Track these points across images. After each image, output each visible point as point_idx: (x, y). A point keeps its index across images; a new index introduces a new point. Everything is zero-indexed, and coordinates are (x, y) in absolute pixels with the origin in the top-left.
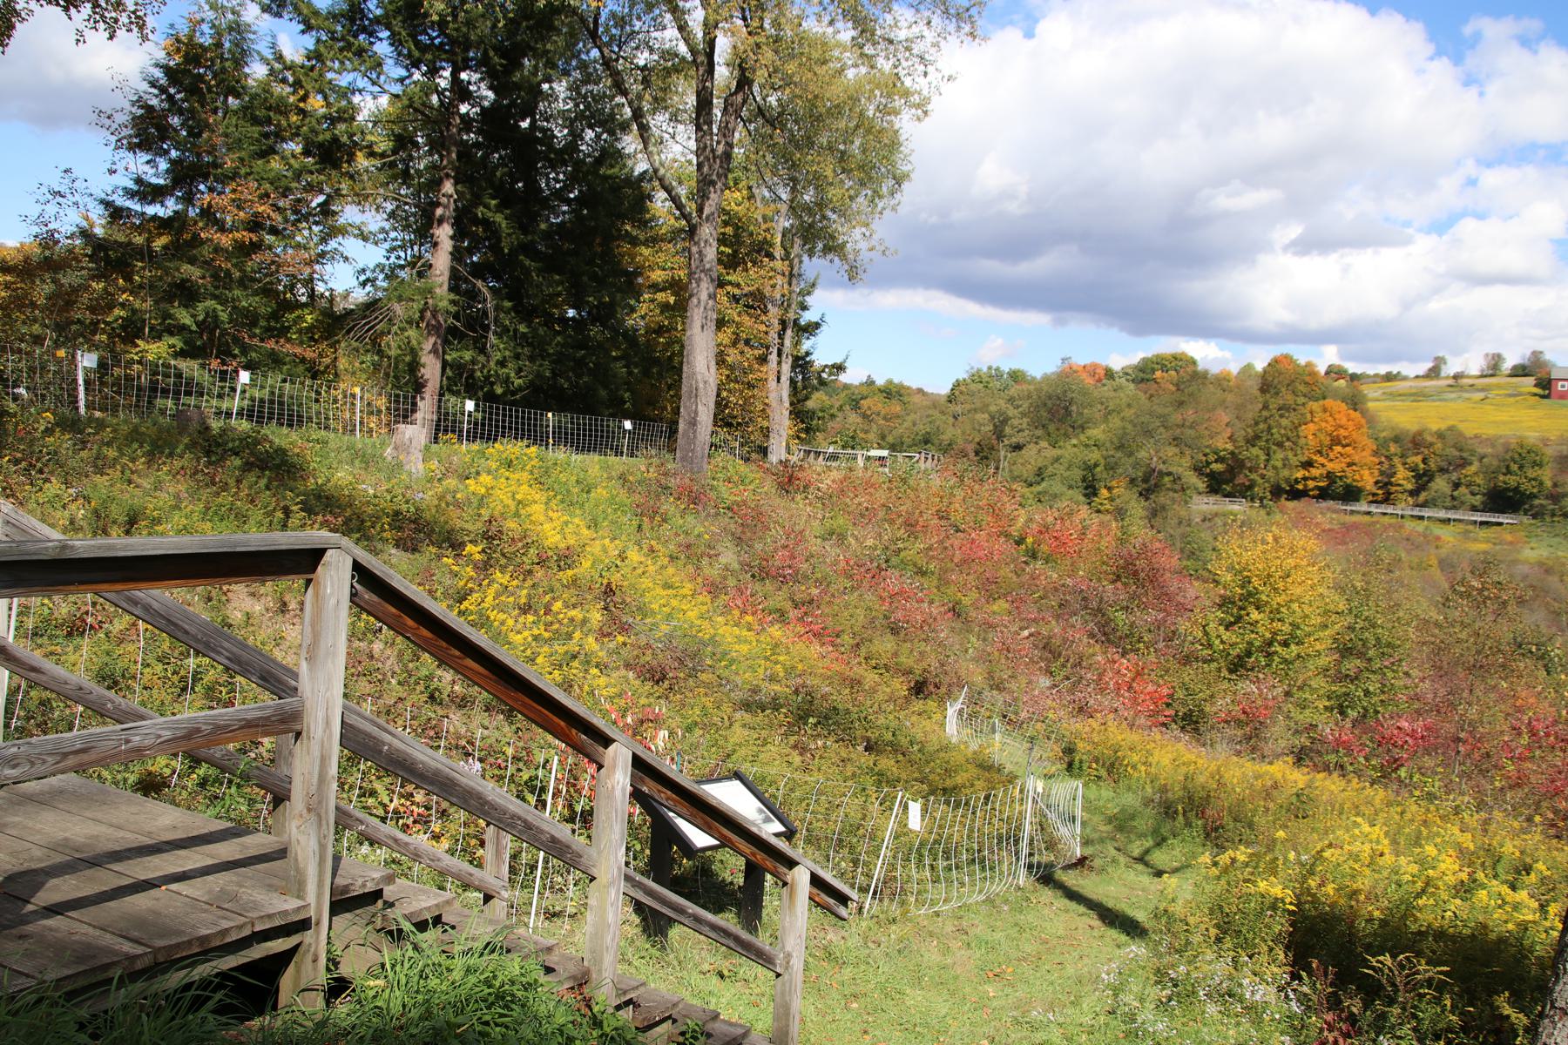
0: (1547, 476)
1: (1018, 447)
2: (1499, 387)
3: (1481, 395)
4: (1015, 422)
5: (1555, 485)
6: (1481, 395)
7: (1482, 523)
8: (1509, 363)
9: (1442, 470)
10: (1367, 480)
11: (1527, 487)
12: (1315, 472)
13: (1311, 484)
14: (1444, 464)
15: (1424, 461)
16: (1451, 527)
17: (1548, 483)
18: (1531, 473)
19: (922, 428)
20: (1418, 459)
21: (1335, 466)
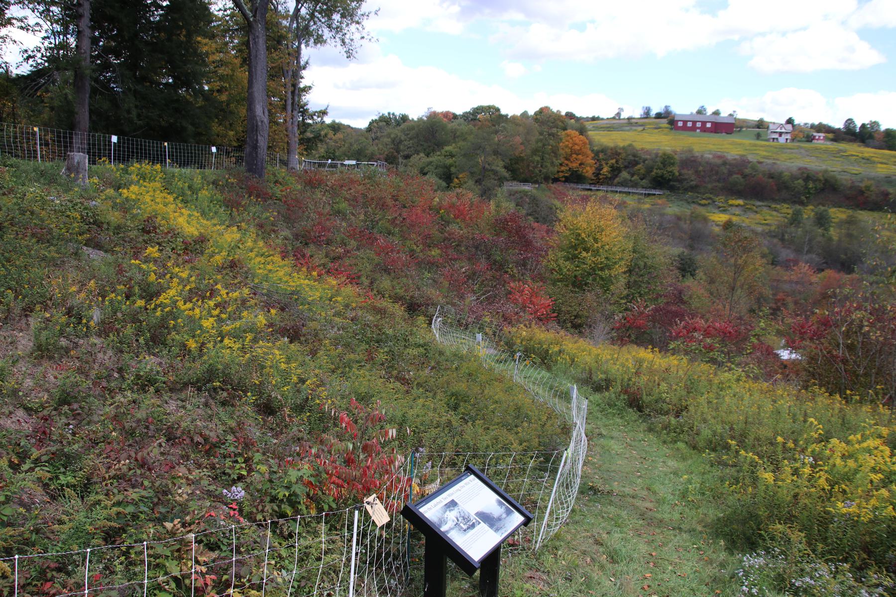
0: (676, 170)
1: (407, 157)
2: (650, 124)
4: (406, 143)
5: (680, 174)
6: (640, 128)
8: (653, 113)
9: (626, 167)
10: (589, 172)
11: (667, 176)
12: (563, 168)
13: (561, 174)
16: (631, 197)
17: (677, 174)
18: (669, 169)
19: (356, 147)
21: (574, 165)
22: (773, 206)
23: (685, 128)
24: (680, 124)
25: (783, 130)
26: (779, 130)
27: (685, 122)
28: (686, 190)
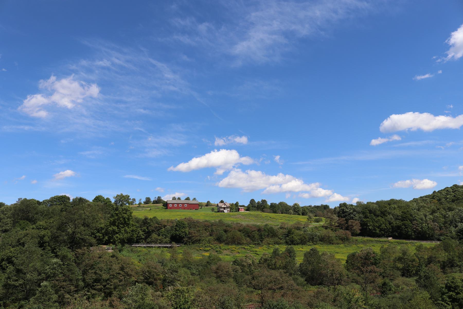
0: (187, 230)
11: (183, 235)
20: (145, 228)
22: (246, 247)
24: (171, 206)
26: (223, 206)
28: (193, 243)
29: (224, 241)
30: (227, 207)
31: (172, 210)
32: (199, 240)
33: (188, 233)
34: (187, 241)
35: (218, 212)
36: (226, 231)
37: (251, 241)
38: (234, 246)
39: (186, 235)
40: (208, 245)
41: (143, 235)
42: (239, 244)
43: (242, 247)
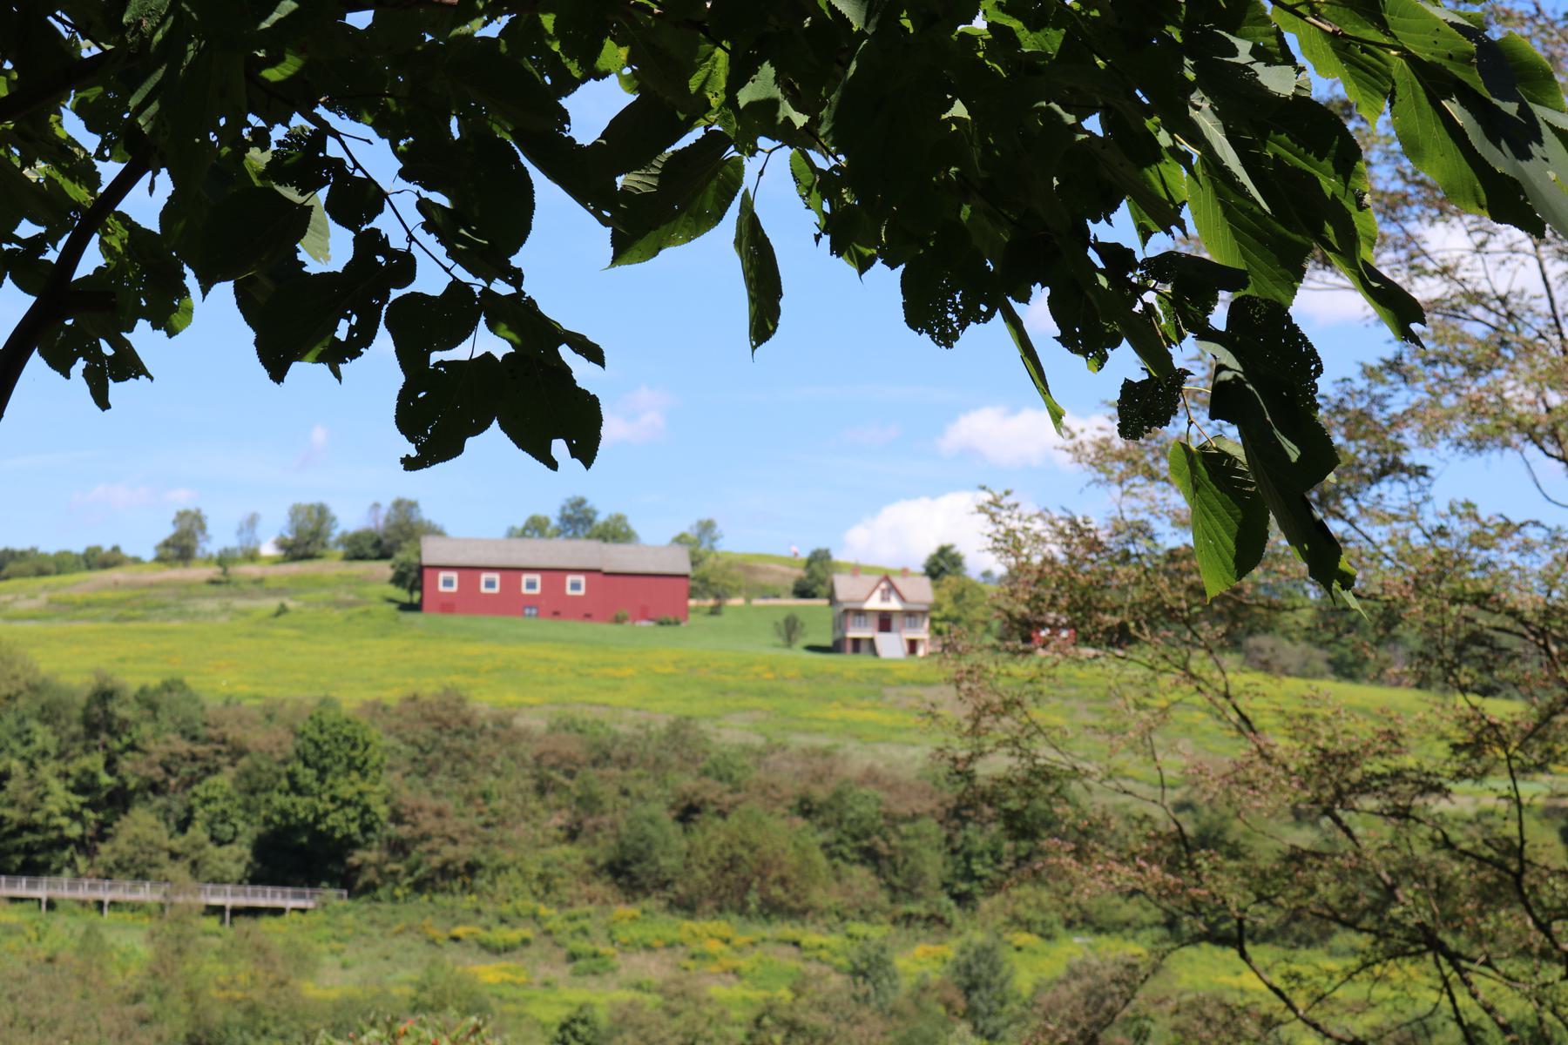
3: (273, 604)
7: (236, 912)
11: (340, 822)
14: (157, 774)
15: (110, 766)
18: (346, 790)
23: (468, 602)
25: (894, 604)
26: (875, 603)
27: (470, 571)
29: (664, 885)
30: (910, 614)
31: (456, 620)
32: (472, 868)
33: (383, 811)
34: (378, 867)
35: (836, 648)
36: (688, 813)
37: (883, 898)
38: (720, 927)
39: (366, 828)
40: (527, 903)
41: (75, 816)
42: (772, 910)
43: (788, 930)
